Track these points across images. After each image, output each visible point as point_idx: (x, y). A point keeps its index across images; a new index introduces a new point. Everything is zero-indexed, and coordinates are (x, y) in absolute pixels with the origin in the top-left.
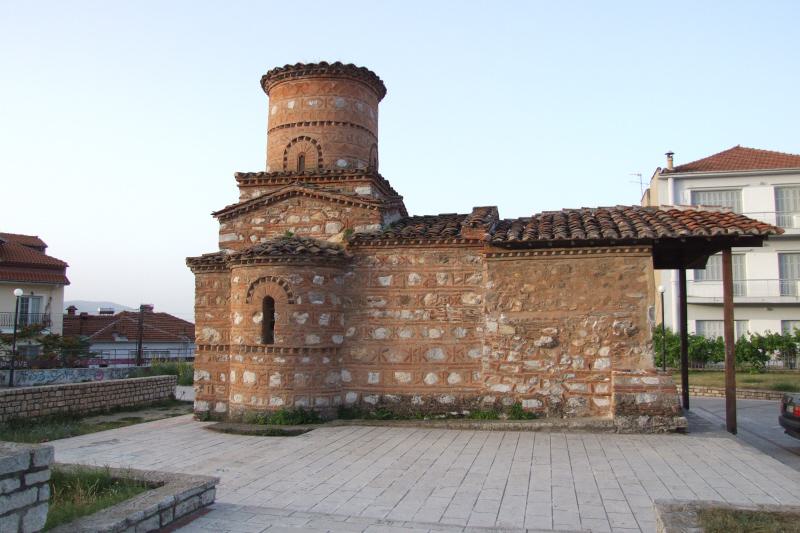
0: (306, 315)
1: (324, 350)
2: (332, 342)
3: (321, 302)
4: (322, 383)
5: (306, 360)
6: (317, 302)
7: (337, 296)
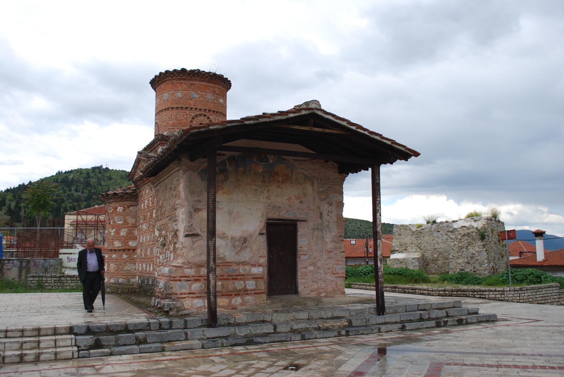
0: (114, 230)
1: (124, 250)
3: (122, 222)
4: (122, 270)
5: (114, 256)
7: (132, 218)
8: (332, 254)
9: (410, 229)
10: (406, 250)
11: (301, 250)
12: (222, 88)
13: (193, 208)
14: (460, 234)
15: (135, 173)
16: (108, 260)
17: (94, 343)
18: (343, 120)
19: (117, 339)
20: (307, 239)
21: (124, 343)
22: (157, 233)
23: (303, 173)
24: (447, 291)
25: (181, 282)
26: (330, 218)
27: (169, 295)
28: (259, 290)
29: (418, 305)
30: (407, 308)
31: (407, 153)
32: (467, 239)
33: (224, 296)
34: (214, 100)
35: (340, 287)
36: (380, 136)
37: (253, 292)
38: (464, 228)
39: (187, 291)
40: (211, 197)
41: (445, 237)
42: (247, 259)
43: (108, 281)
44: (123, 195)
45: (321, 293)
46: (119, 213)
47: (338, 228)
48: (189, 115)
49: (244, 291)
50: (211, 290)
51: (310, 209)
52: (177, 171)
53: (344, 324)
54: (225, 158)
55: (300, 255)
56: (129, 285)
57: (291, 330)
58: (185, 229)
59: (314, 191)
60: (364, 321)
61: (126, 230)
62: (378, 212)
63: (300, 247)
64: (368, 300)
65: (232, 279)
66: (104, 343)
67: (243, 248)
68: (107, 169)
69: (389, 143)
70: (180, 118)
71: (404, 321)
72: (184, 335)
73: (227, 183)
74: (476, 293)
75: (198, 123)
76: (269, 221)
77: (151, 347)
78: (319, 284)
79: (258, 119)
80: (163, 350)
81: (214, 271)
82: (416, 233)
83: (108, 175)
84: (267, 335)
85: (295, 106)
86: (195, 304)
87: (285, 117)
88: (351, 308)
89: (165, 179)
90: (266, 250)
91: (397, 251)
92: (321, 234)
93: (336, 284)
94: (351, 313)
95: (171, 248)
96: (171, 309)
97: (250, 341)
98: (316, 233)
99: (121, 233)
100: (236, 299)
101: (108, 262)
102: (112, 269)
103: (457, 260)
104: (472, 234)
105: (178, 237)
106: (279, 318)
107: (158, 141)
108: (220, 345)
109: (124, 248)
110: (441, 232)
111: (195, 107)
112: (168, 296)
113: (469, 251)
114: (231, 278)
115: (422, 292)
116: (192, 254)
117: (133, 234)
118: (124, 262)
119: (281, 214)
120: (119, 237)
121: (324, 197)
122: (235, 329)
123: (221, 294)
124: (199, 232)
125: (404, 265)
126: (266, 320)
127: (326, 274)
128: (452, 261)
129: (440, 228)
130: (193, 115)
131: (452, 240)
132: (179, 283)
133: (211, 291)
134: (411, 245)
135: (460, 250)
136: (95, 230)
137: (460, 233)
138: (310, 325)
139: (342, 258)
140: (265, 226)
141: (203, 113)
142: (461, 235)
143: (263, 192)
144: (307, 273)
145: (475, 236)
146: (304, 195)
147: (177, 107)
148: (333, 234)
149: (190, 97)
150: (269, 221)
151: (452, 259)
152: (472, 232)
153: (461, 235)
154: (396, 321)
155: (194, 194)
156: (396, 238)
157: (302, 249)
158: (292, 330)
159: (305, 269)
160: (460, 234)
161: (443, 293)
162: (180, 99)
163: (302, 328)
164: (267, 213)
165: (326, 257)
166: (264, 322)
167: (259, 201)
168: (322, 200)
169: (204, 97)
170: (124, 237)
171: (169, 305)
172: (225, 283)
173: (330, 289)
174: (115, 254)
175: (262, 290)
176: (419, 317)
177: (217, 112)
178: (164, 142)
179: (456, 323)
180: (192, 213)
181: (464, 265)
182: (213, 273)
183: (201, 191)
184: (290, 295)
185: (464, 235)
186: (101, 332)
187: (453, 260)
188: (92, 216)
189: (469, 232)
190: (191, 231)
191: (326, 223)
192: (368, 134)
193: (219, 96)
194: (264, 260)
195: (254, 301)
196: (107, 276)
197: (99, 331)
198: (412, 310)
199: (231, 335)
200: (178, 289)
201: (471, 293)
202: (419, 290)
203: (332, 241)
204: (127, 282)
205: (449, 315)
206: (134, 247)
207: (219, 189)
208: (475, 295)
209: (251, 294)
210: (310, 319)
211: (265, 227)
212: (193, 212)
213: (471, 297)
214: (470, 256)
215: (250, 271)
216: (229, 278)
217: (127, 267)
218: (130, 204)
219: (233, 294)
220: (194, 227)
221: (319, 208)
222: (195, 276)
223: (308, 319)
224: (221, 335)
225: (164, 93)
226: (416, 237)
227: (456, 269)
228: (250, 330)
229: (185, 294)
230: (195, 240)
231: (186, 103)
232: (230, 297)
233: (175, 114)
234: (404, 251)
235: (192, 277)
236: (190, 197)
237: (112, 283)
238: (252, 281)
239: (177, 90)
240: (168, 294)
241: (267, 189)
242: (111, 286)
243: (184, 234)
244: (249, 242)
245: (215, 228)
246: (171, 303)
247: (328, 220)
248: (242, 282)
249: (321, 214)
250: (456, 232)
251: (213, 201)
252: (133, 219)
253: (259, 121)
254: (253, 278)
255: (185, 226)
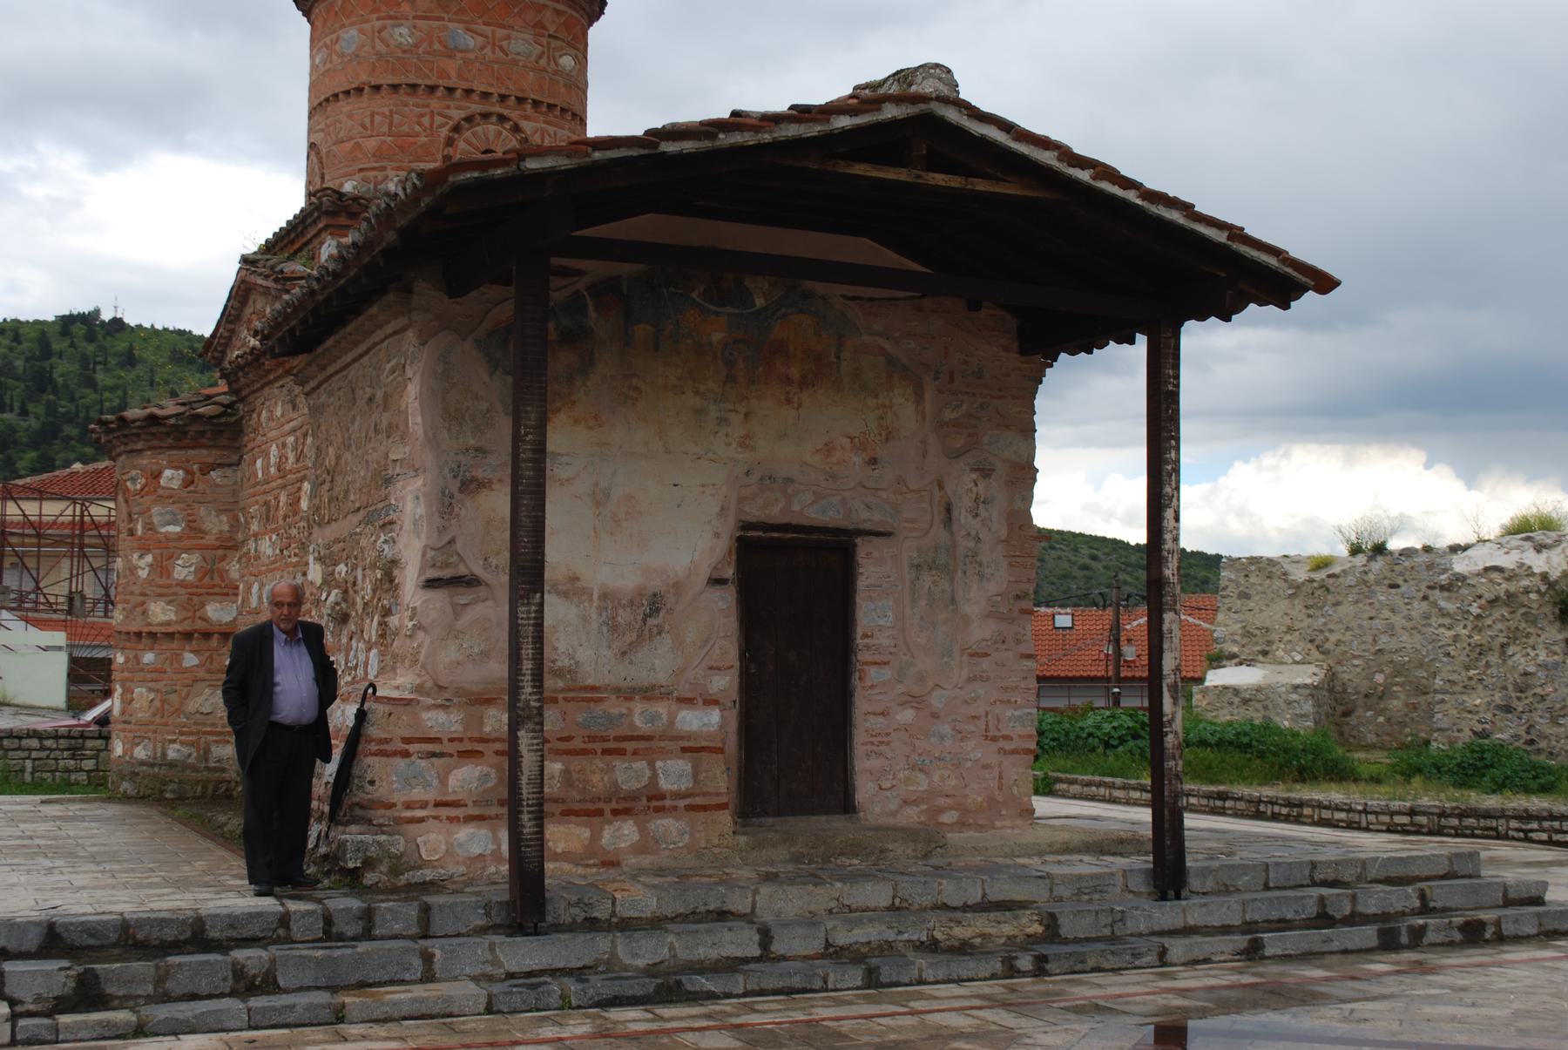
0: (149, 558)
1: (188, 636)
2: (205, 619)
3: (178, 529)
4: (178, 711)
5: (148, 657)
6: (171, 529)
7: (220, 512)
8: (985, 664)
9: (1285, 574)
10: (1265, 653)
11: (868, 647)
12: (569, 11)
13: (455, 477)
14: (1480, 597)
15: (230, 338)
16: (126, 674)
17: (76, 989)
18: (1044, 143)
19: (162, 972)
20: (891, 603)
21: (189, 989)
22: (315, 573)
23: (883, 349)
24: (1424, 813)
25: (407, 760)
26: (983, 525)
27: (363, 807)
28: (705, 794)
29: (1314, 865)
30: (1272, 875)
31: (1286, 277)
32: (1504, 619)
33: (573, 818)
34: (540, 57)
35: (1015, 790)
36: (1187, 208)
37: (682, 803)
38: (1495, 576)
39: (431, 795)
40: (526, 434)
41: (1419, 608)
42: (662, 678)
43: (125, 752)
44: (185, 425)
45: (942, 810)
46: (167, 493)
47: (1011, 565)
48: (440, 114)
49: (650, 799)
50: (524, 792)
51: (904, 489)
52: (395, 333)
53: (1030, 931)
54: (581, 285)
55: (867, 663)
56: (207, 768)
57: (826, 948)
58: (424, 555)
59: (924, 418)
60: (1105, 919)
61: (195, 558)
62: (1168, 506)
63: (865, 636)
64: (1122, 841)
65: (606, 752)
66: (111, 989)
67: (645, 635)
68: (117, 323)
69: (1220, 237)
70: (405, 128)
71: (1256, 922)
72: (417, 963)
73: (589, 384)
74: (1535, 825)
75: (477, 149)
76: (750, 534)
77: (292, 1007)
78: (936, 778)
79: (713, 137)
80: (338, 1018)
81: (537, 719)
82: (1308, 588)
83: (122, 346)
84: (732, 965)
85: (855, 88)
86: (461, 845)
87: (819, 128)
88: (1056, 870)
89: (348, 366)
90: (736, 644)
91: (1232, 656)
92: (947, 587)
93: (1001, 777)
94: (1055, 888)
95: (372, 628)
96: (369, 864)
97: (670, 990)
98: (927, 580)
99: (178, 569)
100: (620, 828)
101: (127, 680)
102: (141, 708)
103: (1465, 697)
104: (1523, 599)
105: (397, 588)
106: (781, 904)
107: (319, 218)
108: (554, 1000)
109: (187, 626)
110: (1404, 588)
111: (465, 85)
112: (358, 812)
113: (1510, 662)
114: (598, 746)
115: (1326, 814)
116: (450, 654)
117: (223, 574)
118: (190, 682)
119: (796, 507)
120: (169, 586)
121: (959, 443)
122: (613, 942)
123: (563, 807)
124: (478, 570)
125: (1257, 710)
126: (733, 908)
127: (962, 740)
128: (1442, 701)
129: (1401, 574)
130: (457, 115)
131: (1447, 621)
132: (400, 763)
133: (525, 796)
134: (1288, 637)
135: (1477, 660)
136: (72, 557)
137: (1480, 591)
138: (900, 933)
139: (1025, 678)
140: (734, 553)
141: (498, 109)
142: (1483, 601)
143: (726, 419)
144: (888, 734)
145: (1535, 605)
146: (884, 433)
147: (397, 82)
148: (993, 587)
149: (445, 46)
150: (750, 534)
151: (1446, 692)
152: (1527, 591)
153: (1483, 601)
154: (1226, 923)
155: (460, 424)
156: (1229, 609)
157: (876, 642)
158: (831, 950)
159: (881, 719)
160: (1480, 597)
161: (1405, 820)
162: (404, 52)
163: (869, 943)
164: (741, 500)
165: (965, 673)
166: (722, 915)
167: (710, 455)
168: (955, 455)
169: (501, 48)
170: (186, 587)
171: (360, 847)
172: (577, 768)
173: (976, 797)
174: (151, 649)
175: (718, 794)
176: (1315, 909)
177: (551, 107)
178: (343, 220)
179: (1458, 936)
180: (452, 497)
181: (1489, 716)
182: (531, 726)
183: (488, 411)
184: (823, 818)
185: (1493, 602)
186: (102, 947)
187: (1447, 697)
188: (65, 504)
189: (1512, 589)
190: (447, 565)
191: (965, 544)
192: (1139, 202)
193: (559, 43)
194: (725, 683)
195: (687, 838)
196: (122, 734)
197: (91, 942)
198: (1292, 883)
199: (598, 962)
200: (395, 786)
201: (1514, 824)
202: (1313, 807)
203: (990, 615)
204: (196, 758)
205: (1432, 904)
206: (227, 624)
207: (558, 404)
208: (1532, 831)
209: (675, 808)
210: (898, 909)
211: (734, 557)
212: (456, 493)
213: (1514, 839)
214: (1516, 684)
215: (672, 723)
216: (590, 746)
217: (199, 700)
218: (210, 460)
219: (607, 808)
220: (459, 550)
221: (941, 487)
222: (461, 740)
223: (892, 908)
224: (561, 965)
225: (343, 26)
226: (1306, 607)
227: (1459, 731)
228: (671, 948)
229: (424, 805)
230: (463, 600)
231: (431, 70)
232: (597, 820)
233: (386, 110)
234: (1260, 658)
235: (451, 740)
236: (445, 434)
237: (142, 763)
238: (680, 762)
239: (396, 18)
240: (357, 804)
241: (744, 410)
242: (137, 774)
243: (423, 578)
244: (671, 611)
245: (543, 554)
246: (368, 838)
247: (973, 533)
248: (641, 765)
249: (949, 510)
250: (1464, 591)
251: (535, 451)
252: (224, 518)
253: (717, 143)
254: (685, 750)
255: (426, 546)
